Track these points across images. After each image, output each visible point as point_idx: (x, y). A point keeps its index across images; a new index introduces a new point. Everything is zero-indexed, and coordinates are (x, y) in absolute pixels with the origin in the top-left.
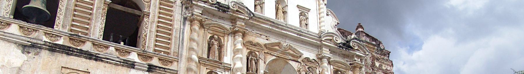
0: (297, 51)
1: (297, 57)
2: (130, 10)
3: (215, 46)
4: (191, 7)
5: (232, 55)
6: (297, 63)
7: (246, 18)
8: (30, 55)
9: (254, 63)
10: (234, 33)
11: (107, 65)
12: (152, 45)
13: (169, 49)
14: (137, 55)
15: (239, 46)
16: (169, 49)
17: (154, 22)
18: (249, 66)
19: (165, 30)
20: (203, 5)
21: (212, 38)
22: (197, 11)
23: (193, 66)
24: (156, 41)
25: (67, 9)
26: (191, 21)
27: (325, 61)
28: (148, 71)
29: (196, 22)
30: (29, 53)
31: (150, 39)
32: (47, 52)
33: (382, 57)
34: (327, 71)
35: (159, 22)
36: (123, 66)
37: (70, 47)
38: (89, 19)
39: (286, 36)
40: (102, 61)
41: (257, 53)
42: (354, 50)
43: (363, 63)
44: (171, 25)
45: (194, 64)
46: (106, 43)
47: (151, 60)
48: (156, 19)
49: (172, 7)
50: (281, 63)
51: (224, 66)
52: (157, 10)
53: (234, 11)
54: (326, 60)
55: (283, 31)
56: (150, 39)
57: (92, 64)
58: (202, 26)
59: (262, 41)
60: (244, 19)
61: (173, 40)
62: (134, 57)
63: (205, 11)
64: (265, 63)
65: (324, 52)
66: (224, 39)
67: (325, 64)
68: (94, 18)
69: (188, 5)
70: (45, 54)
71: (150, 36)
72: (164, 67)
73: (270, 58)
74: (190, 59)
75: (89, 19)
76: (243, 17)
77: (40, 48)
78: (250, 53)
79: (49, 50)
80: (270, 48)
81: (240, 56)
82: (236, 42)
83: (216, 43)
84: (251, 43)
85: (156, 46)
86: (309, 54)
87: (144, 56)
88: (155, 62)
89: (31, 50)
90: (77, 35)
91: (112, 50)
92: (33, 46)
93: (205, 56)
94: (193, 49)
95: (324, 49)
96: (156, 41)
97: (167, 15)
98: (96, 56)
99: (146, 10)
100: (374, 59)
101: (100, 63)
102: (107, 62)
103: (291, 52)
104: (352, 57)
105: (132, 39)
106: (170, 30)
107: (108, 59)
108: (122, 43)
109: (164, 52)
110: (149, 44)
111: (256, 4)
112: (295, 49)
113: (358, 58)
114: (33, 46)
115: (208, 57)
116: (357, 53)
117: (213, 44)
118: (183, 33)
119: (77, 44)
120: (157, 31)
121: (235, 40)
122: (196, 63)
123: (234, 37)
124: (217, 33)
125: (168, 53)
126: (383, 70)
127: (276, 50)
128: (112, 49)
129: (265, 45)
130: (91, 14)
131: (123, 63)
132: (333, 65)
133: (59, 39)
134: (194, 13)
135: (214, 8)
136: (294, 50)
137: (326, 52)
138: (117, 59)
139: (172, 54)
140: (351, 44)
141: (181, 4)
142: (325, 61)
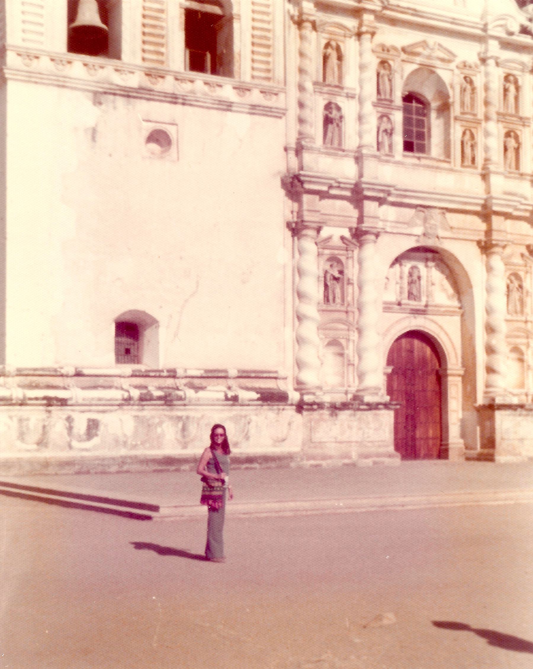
8: (103, 107)
9: (386, 79)
21: (327, 45)
40: (191, 105)
51: (347, 94)
73: (410, 68)
86: (467, 52)
93: (321, 79)
97: (264, 13)
137: (494, 47)
142: (491, 62)
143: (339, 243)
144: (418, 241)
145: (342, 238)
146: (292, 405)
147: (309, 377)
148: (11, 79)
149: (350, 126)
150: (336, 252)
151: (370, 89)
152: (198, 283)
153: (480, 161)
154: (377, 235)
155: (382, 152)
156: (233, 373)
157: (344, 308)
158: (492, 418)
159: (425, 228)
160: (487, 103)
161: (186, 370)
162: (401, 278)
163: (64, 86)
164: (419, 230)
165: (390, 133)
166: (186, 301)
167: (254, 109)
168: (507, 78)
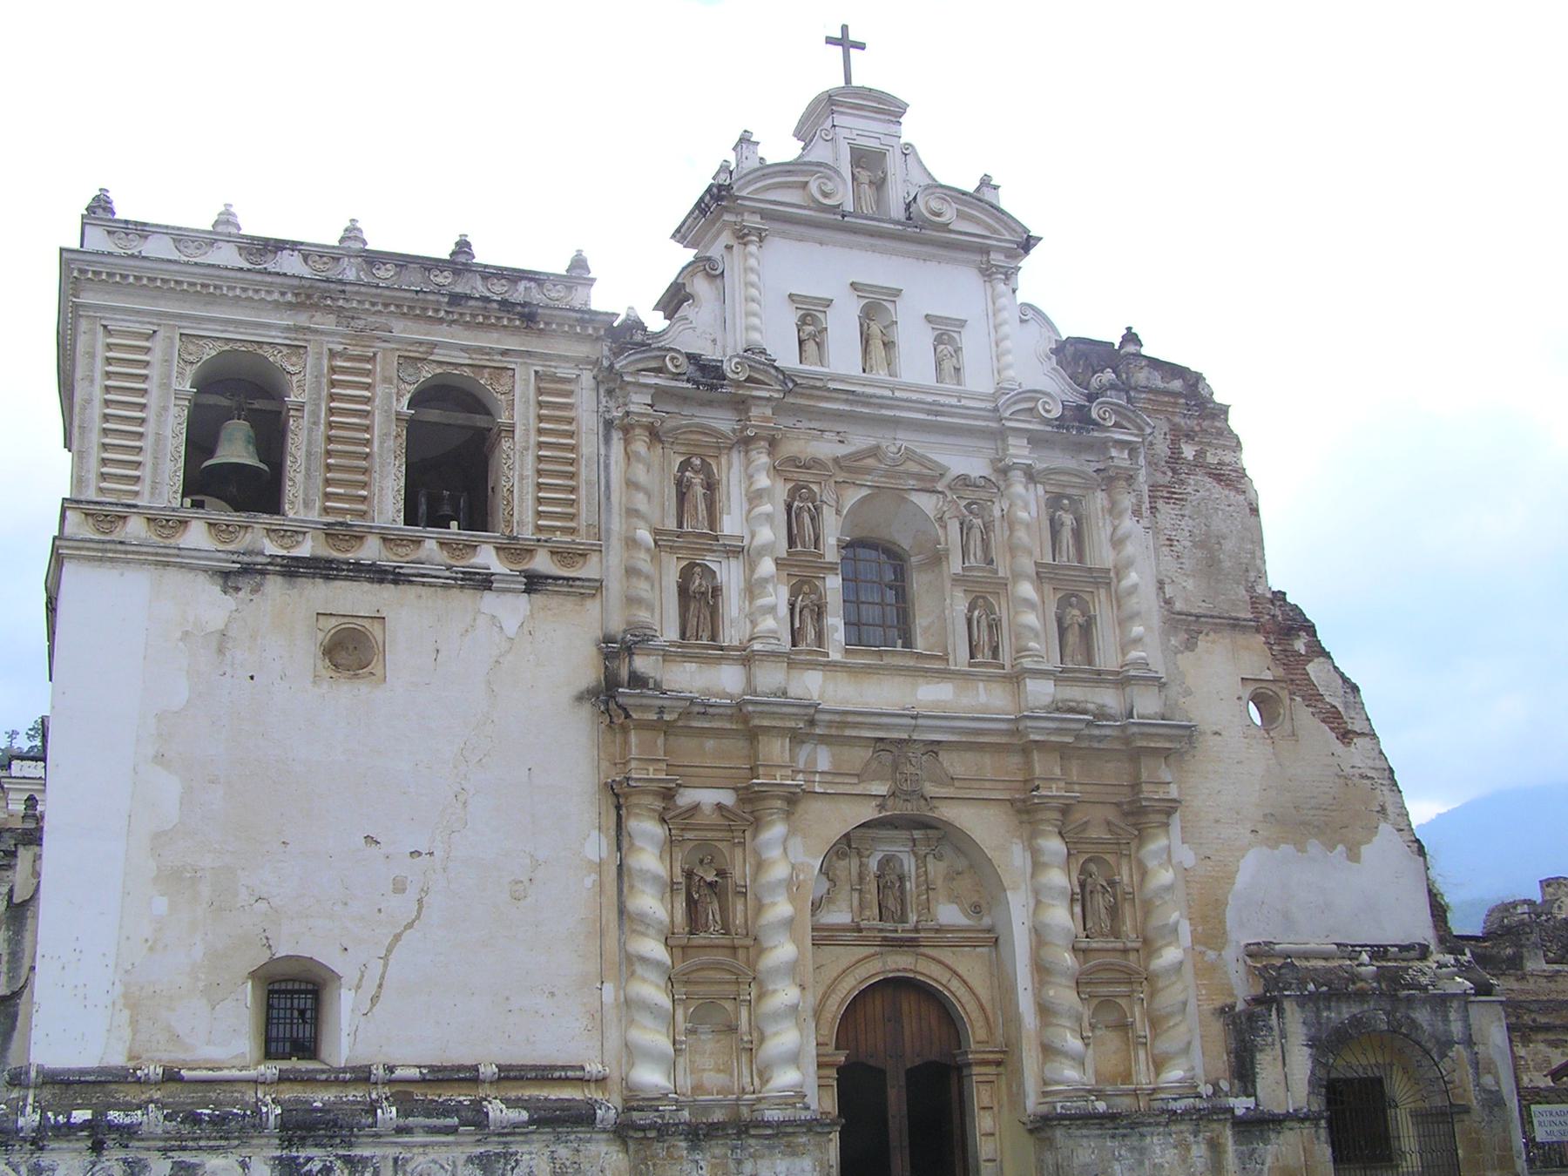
0: (930, 460)
1: (934, 479)
2: (460, 418)
3: (695, 490)
4: (621, 388)
5: (746, 506)
6: (934, 497)
7: (776, 395)
8: (241, 594)
9: (807, 520)
10: (746, 443)
11: (420, 590)
12: (529, 517)
13: (572, 517)
14: (493, 552)
15: (763, 481)
16: (572, 517)
17: (527, 449)
18: (795, 531)
19: (559, 466)
20: (652, 380)
21: (684, 466)
22: (639, 402)
23: (643, 561)
24: (540, 501)
25: (309, 454)
26: (627, 430)
27: (1017, 475)
28: (528, 591)
29: (638, 431)
30: (238, 589)
31: (521, 500)
32: (279, 579)
33: (1205, 424)
34: (1026, 507)
35: (540, 445)
36: (462, 587)
37: (331, 561)
38: (365, 471)
39: (896, 423)
41: (815, 488)
42: (1106, 429)
43: (1142, 461)
44: (572, 448)
45: (643, 555)
46: (416, 531)
47: (532, 557)
48: (533, 438)
49: (569, 394)
52: (533, 411)
53: (738, 384)
54: (1019, 473)
55: (884, 412)
56: (521, 500)
57: (388, 592)
58: (654, 435)
59: (826, 449)
60: (769, 399)
61: (583, 492)
62: (487, 558)
63: (660, 393)
64: (838, 512)
65: (1012, 451)
66: (719, 464)
67: (1019, 488)
68: (377, 468)
69: (612, 385)
70: (274, 586)
71: (521, 490)
72: (566, 574)
73: (852, 497)
74: (631, 543)
75: (365, 471)
76: (766, 394)
77: (263, 573)
78: (794, 493)
79: (282, 574)
80: (850, 467)
81: (767, 508)
82: (751, 470)
83: (697, 480)
84: (793, 461)
85: (539, 514)
87: (512, 549)
88: (542, 563)
89: (246, 583)
90: (341, 524)
91: (431, 548)
92: (247, 570)
93: (671, 524)
94: (637, 511)
95: (1011, 441)
96: (540, 501)
97: (558, 420)
98: (393, 573)
99: (503, 419)
100: (1179, 435)
101: (406, 587)
102: (423, 584)
103: (914, 468)
104: (1102, 447)
105: (478, 514)
106: (572, 462)
107: (423, 576)
108: (454, 524)
109: (563, 530)
110: (520, 513)
111: (804, 336)
112: (922, 456)
113: (1122, 450)
114: (247, 570)
115: (680, 525)
116: (1117, 436)
117: (690, 485)
118: (607, 466)
119: (343, 545)
120: (539, 473)
121: (749, 462)
122: (648, 550)
123: (747, 452)
124: (698, 451)
125: (573, 531)
126: (1207, 466)
127: (868, 471)
128: (431, 546)
129: (836, 460)
130: (367, 456)
133: (300, 538)
134: (633, 408)
135: (685, 385)
136: (922, 461)
137: (1019, 452)
138: (447, 574)
139: (583, 530)
140: (1094, 415)
141: (592, 383)
142: (1017, 475)
143: (715, 819)
144: (882, 807)
145: (720, 807)
146: (604, 1131)
147: (651, 1077)
148: (71, 557)
149: (733, 605)
150: (709, 835)
151: (770, 535)
152: (420, 901)
153: (1006, 656)
154: (793, 799)
155: (802, 647)
156: (488, 1070)
157: (725, 941)
158: (1049, 1143)
159: (895, 781)
160: (1013, 549)
161: (391, 1069)
162: (861, 878)
163: (167, 564)
164: (881, 788)
165: (819, 612)
166: (397, 937)
167: (534, 583)
168: (1054, 502)
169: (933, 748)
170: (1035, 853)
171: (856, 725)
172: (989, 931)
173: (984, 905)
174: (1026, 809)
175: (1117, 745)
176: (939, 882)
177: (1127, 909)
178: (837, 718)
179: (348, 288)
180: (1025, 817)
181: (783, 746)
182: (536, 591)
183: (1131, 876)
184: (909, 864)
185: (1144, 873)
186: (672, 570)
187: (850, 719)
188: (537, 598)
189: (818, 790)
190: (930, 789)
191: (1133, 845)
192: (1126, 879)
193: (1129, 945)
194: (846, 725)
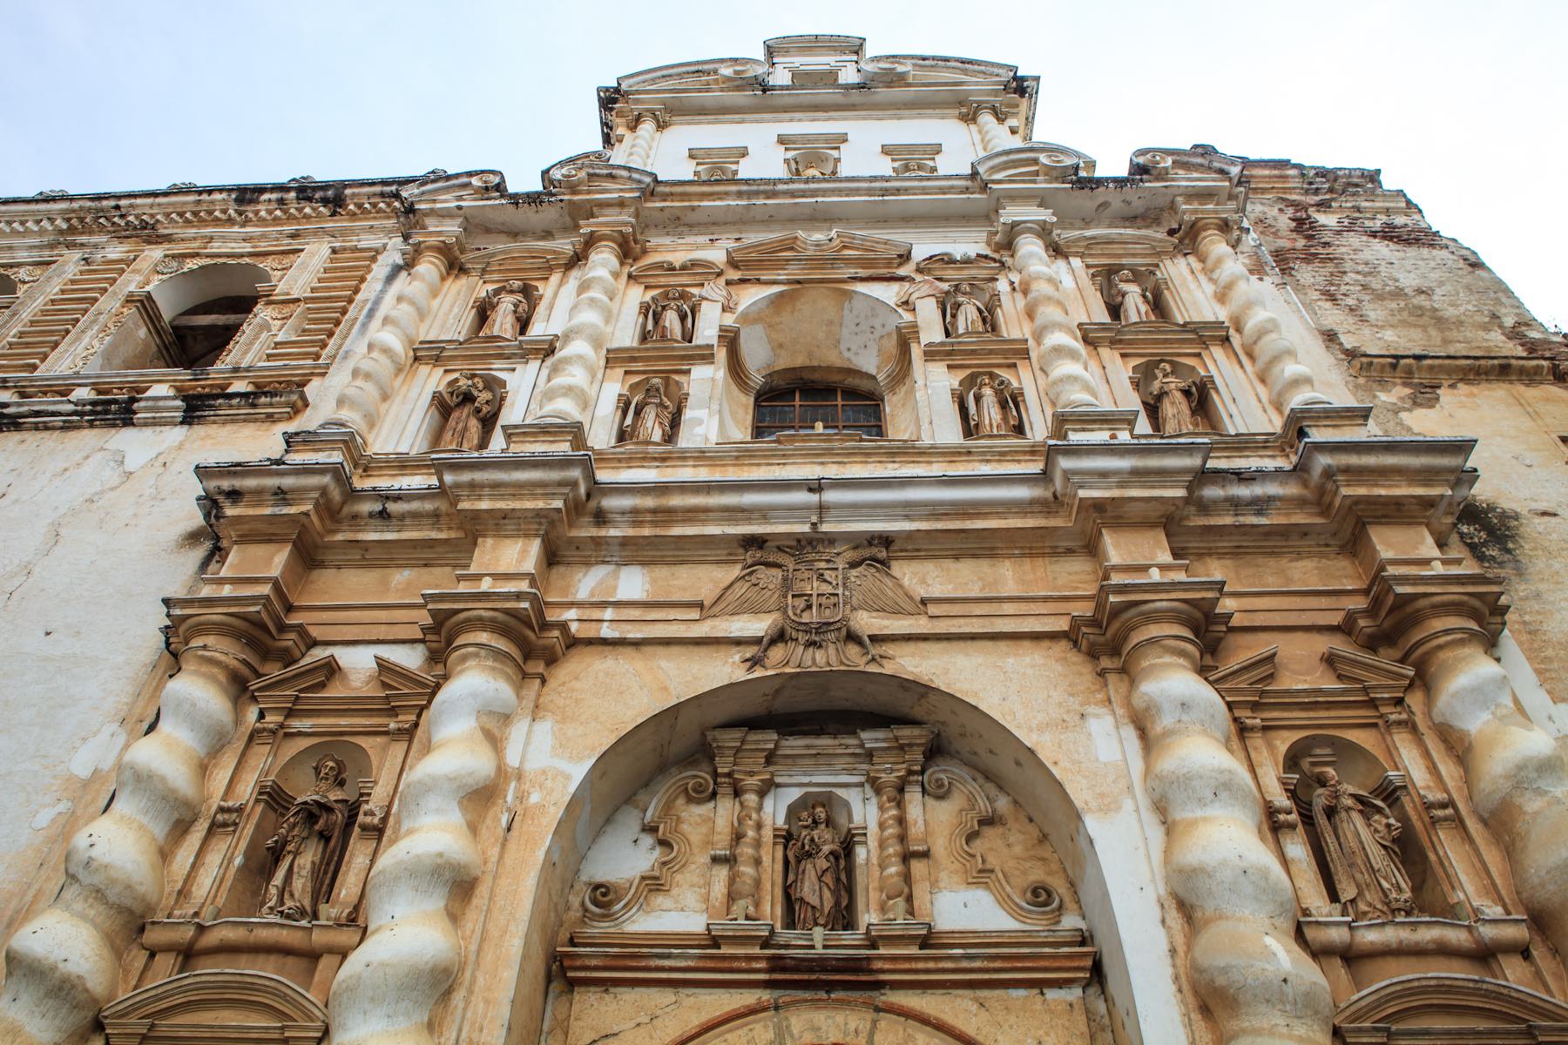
28: (189, 419)
36: (91, 425)
50: (816, 305)
102: (36, 427)
131: (92, 413)
132: (1076, 254)
142: (1030, 248)
164: (758, 626)
169: (879, 551)
170: (1142, 725)
171: (692, 515)
172: (1083, 943)
173: (1060, 887)
174: (1104, 641)
175: (1300, 518)
176: (940, 846)
177: (1450, 850)
178: (649, 502)
179: (123, 202)
180: (1106, 662)
181: (524, 552)
182: (201, 420)
183: (1433, 769)
184: (865, 812)
185: (1459, 747)
186: (433, 380)
187: (676, 501)
188: (199, 430)
189: (606, 632)
190: (866, 622)
191: (1415, 700)
192: (1419, 775)
193: (1488, 932)
194: (666, 515)
